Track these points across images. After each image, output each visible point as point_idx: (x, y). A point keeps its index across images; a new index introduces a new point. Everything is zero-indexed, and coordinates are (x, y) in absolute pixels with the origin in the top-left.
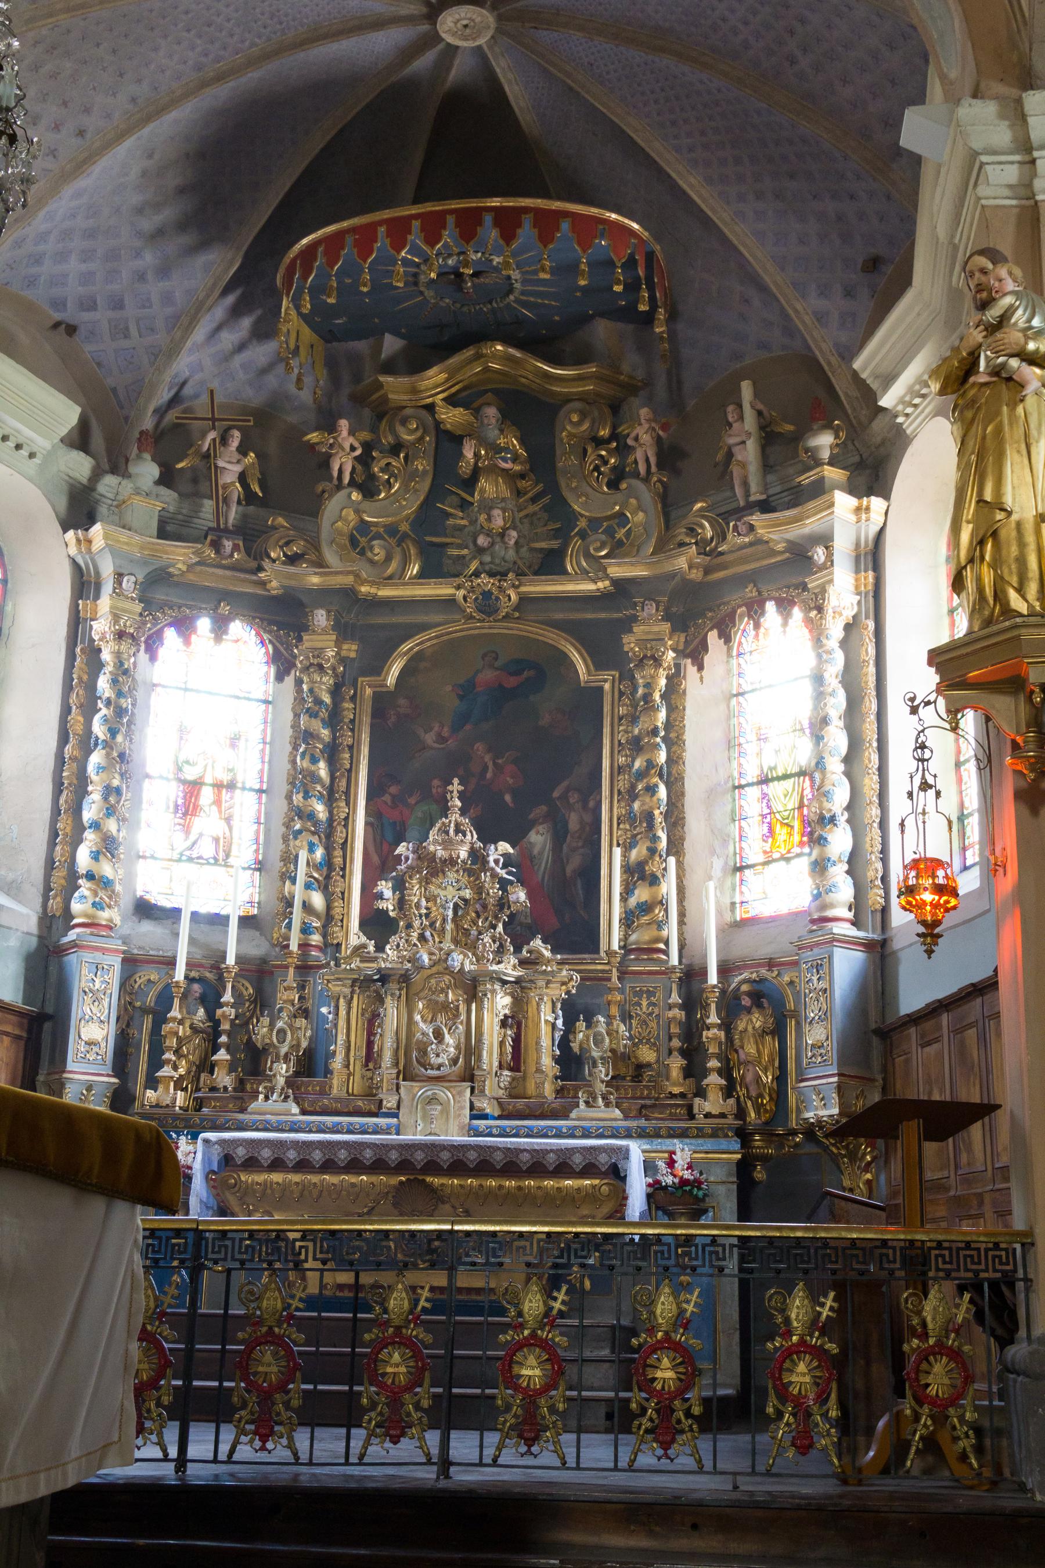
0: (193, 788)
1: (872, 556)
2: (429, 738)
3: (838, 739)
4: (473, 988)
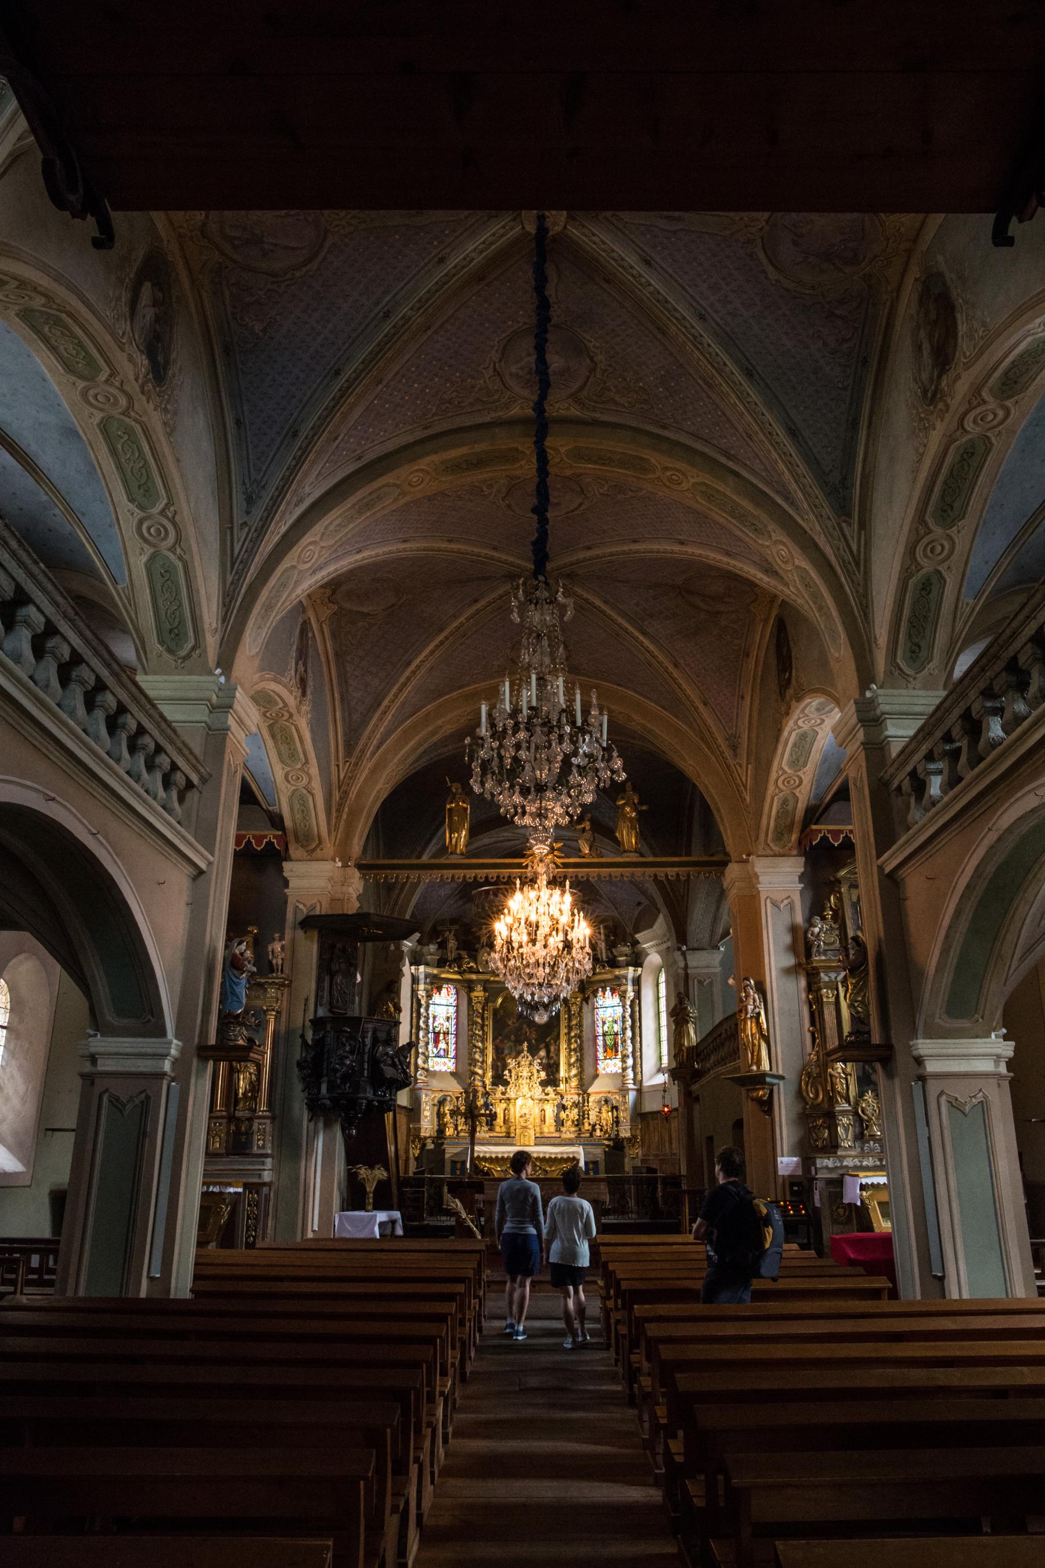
0: (437, 1034)
1: (637, 982)
2: (510, 1023)
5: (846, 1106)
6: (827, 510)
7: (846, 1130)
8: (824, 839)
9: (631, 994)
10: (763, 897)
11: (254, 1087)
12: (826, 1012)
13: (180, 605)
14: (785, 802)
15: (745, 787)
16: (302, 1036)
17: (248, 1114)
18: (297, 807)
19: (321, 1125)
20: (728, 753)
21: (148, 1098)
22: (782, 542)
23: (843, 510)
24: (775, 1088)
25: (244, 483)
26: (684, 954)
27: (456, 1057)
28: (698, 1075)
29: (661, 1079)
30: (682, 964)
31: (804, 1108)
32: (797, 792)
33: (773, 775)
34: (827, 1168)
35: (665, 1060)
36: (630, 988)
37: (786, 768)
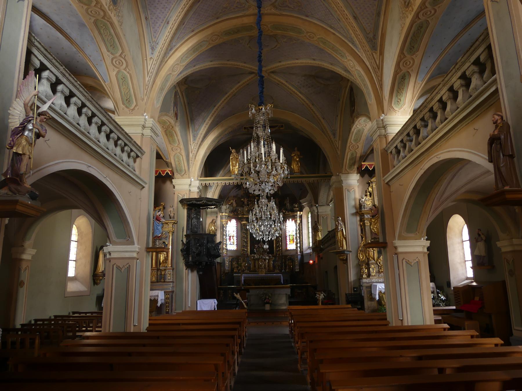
0: (230, 237)
1: (301, 217)
3: (298, 235)
4: (265, 260)
5: (373, 261)
6: (368, 48)
7: (373, 269)
8: (367, 167)
9: (299, 221)
10: (344, 188)
11: (166, 259)
12: (366, 228)
13: (130, 90)
14: (352, 154)
15: (338, 149)
16: (182, 241)
17: (164, 268)
18: (176, 160)
19: (190, 271)
20: (332, 137)
21: (129, 266)
22: (351, 61)
23: (374, 48)
25: (150, 42)
26: (317, 207)
27: (237, 245)
28: (322, 250)
29: (309, 251)
30: (316, 211)
31: (359, 262)
32: (357, 151)
33: (348, 145)
34: (366, 282)
35: (311, 245)
36: (298, 219)
37: (353, 142)
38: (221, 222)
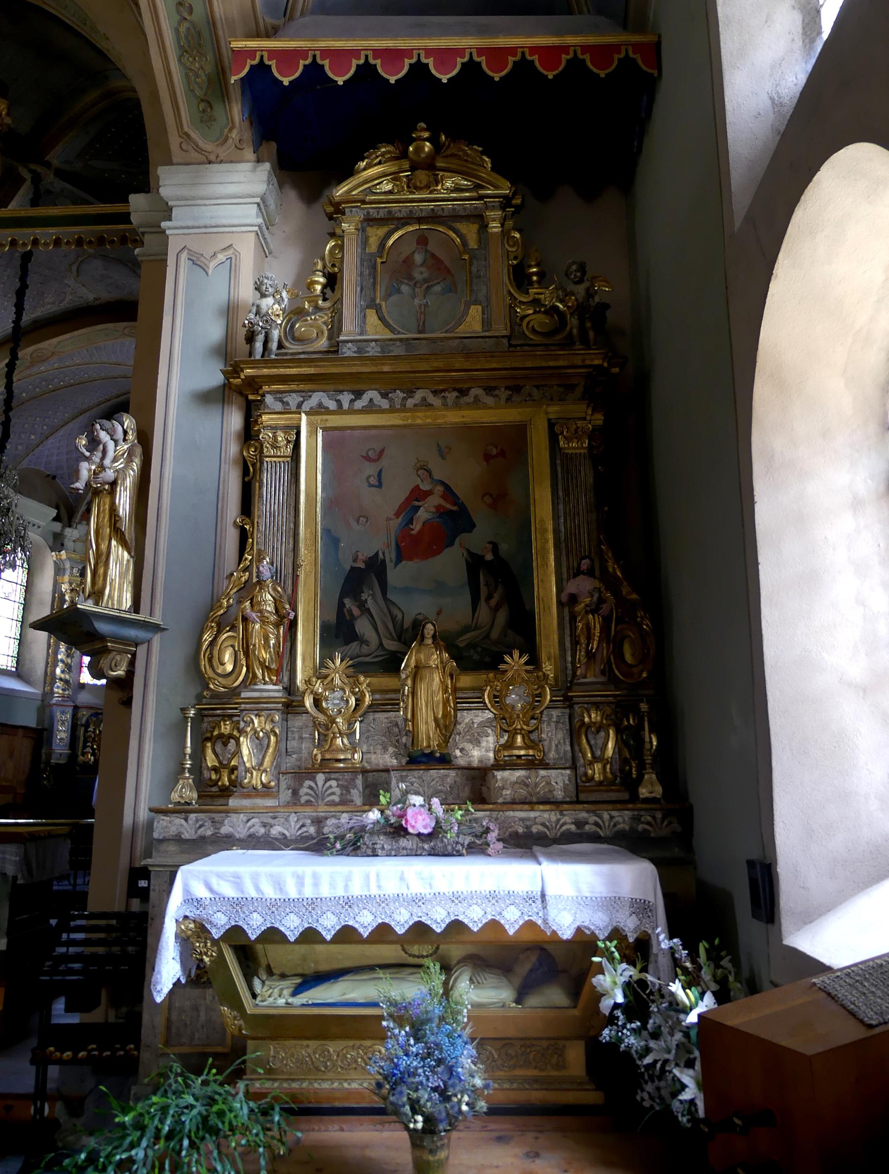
24: (141, 651)
38: (56, 585)
